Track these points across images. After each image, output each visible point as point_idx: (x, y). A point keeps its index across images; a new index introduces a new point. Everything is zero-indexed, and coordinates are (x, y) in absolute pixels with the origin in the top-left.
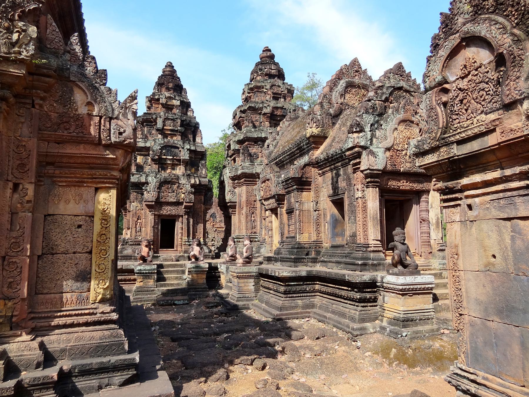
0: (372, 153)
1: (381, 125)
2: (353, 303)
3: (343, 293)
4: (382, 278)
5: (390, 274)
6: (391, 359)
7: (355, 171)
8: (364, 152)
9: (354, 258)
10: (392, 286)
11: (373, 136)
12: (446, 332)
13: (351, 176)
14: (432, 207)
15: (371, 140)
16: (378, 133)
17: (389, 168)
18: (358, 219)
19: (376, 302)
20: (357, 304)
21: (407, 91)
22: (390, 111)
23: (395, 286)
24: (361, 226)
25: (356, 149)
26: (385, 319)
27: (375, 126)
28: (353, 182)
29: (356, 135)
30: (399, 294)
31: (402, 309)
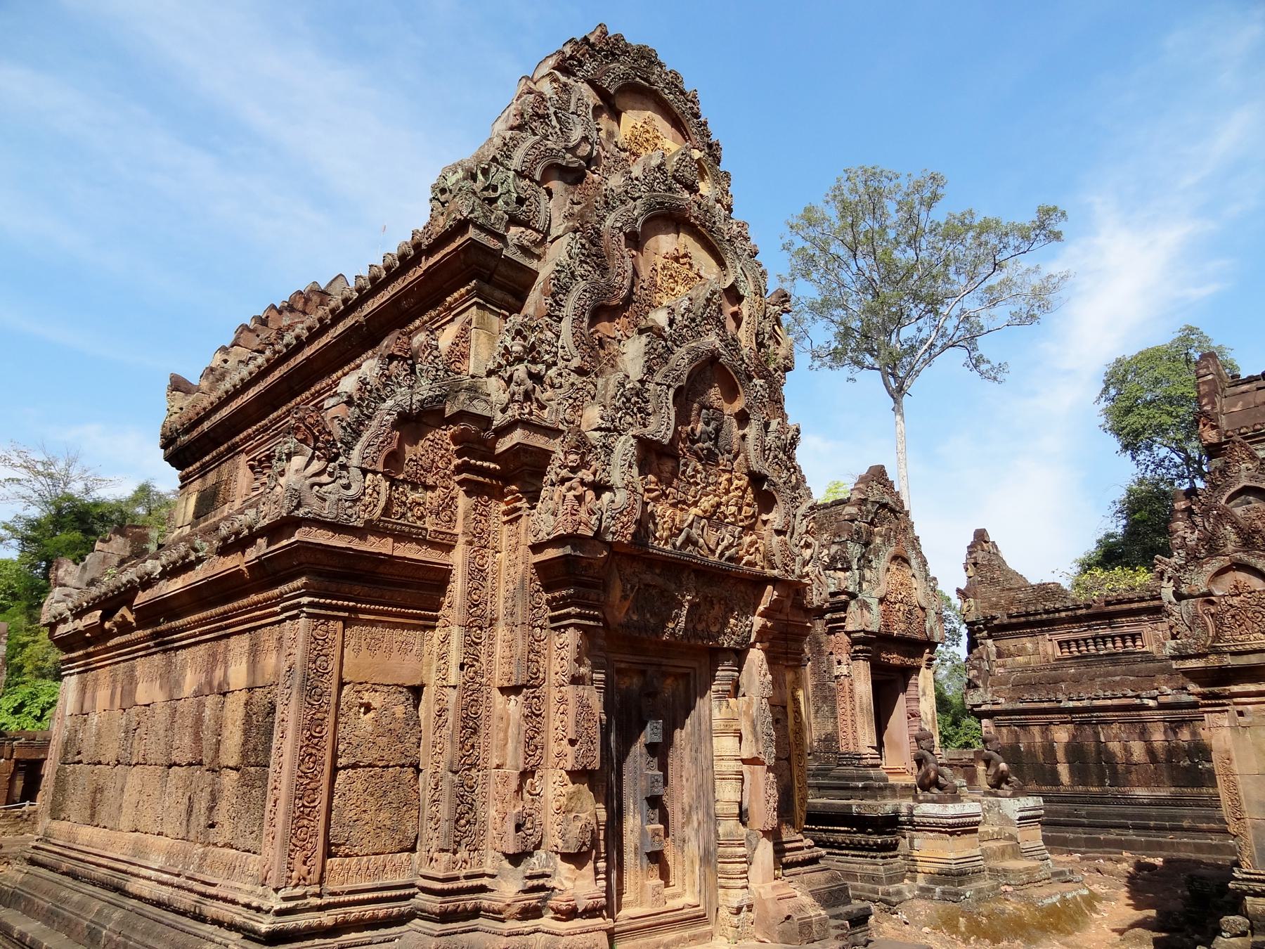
0: (865, 606)
1: (870, 561)
2: (864, 853)
3: (840, 838)
4: (911, 809)
5: (920, 802)
6: (962, 934)
7: (832, 631)
8: (852, 602)
9: (839, 778)
10: (931, 820)
11: (862, 577)
12: (1010, 889)
13: (823, 638)
14: (924, 694)
15: (860, 584)
16: (868, 574)
17: (883, 630)
18: (840, 711)
19: (895, 849)
20: (872, 854)
21: (892, 511)
22: (878, 540)
23: (938, 820)
24: (849, 722)
25: (843, 597)
26: (920, 876)
27: (865, 562)
28: (827, 649)
29: (840, 574)
30: (946, 832)
31: (952, 855)
